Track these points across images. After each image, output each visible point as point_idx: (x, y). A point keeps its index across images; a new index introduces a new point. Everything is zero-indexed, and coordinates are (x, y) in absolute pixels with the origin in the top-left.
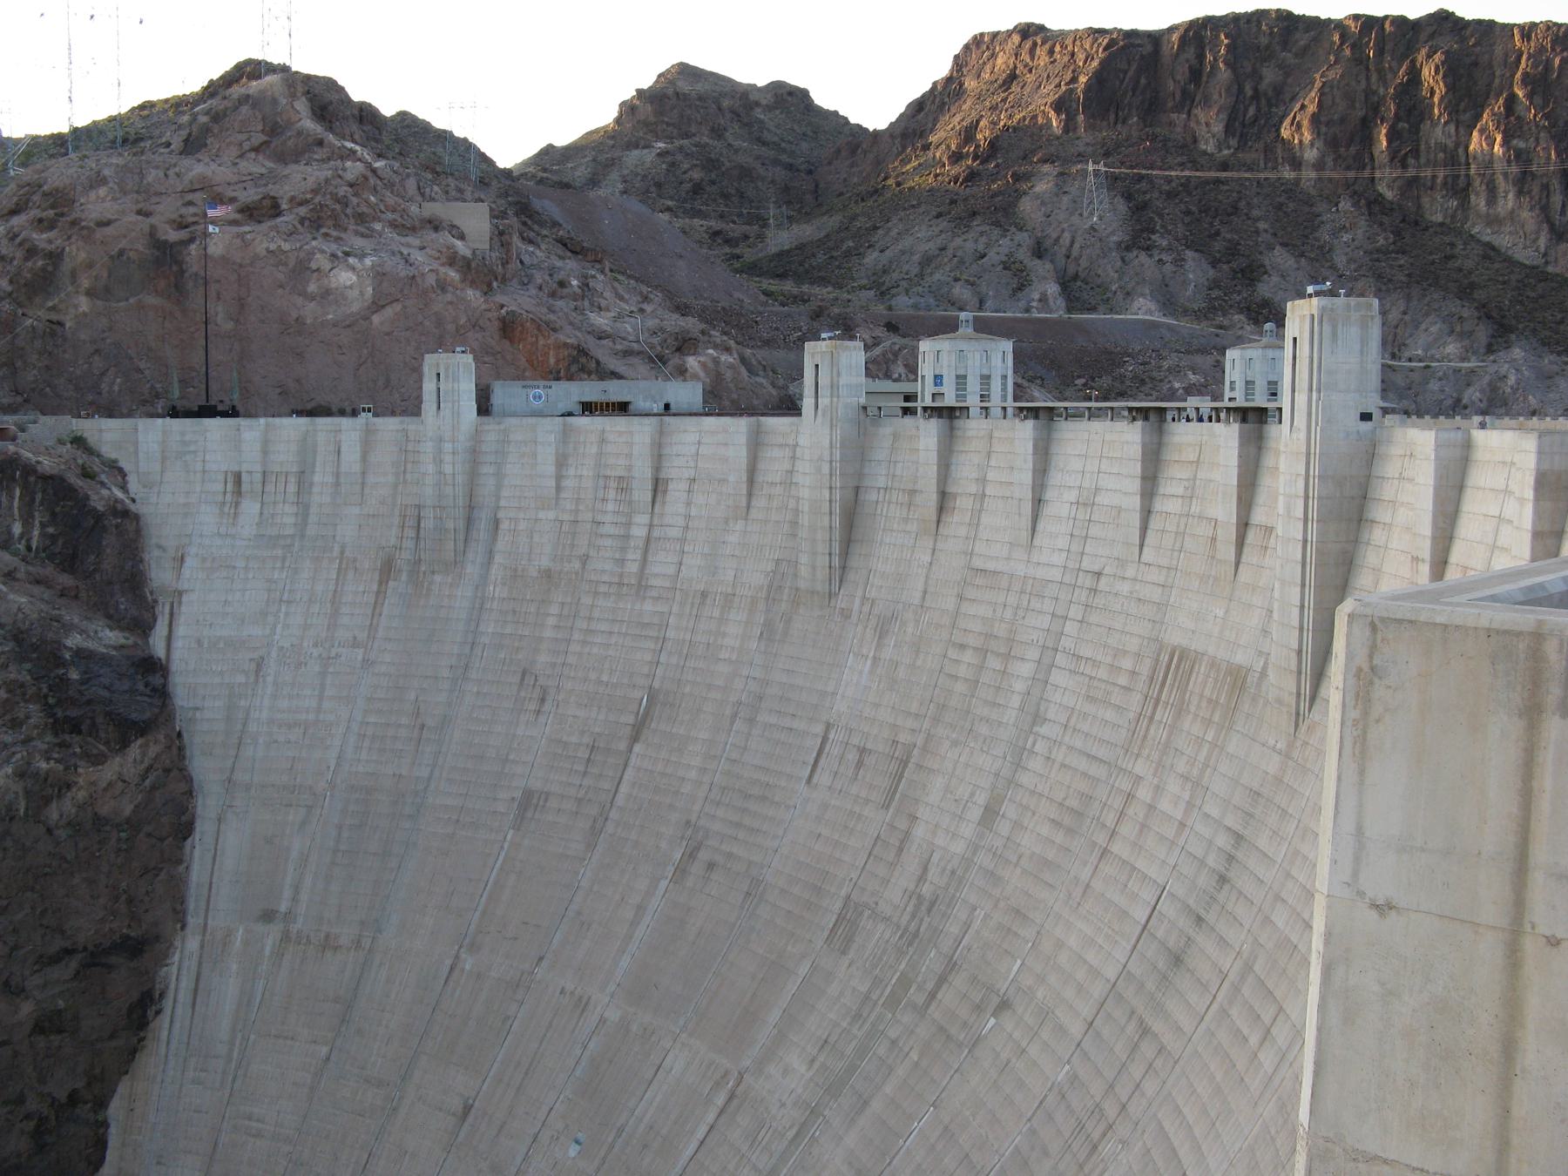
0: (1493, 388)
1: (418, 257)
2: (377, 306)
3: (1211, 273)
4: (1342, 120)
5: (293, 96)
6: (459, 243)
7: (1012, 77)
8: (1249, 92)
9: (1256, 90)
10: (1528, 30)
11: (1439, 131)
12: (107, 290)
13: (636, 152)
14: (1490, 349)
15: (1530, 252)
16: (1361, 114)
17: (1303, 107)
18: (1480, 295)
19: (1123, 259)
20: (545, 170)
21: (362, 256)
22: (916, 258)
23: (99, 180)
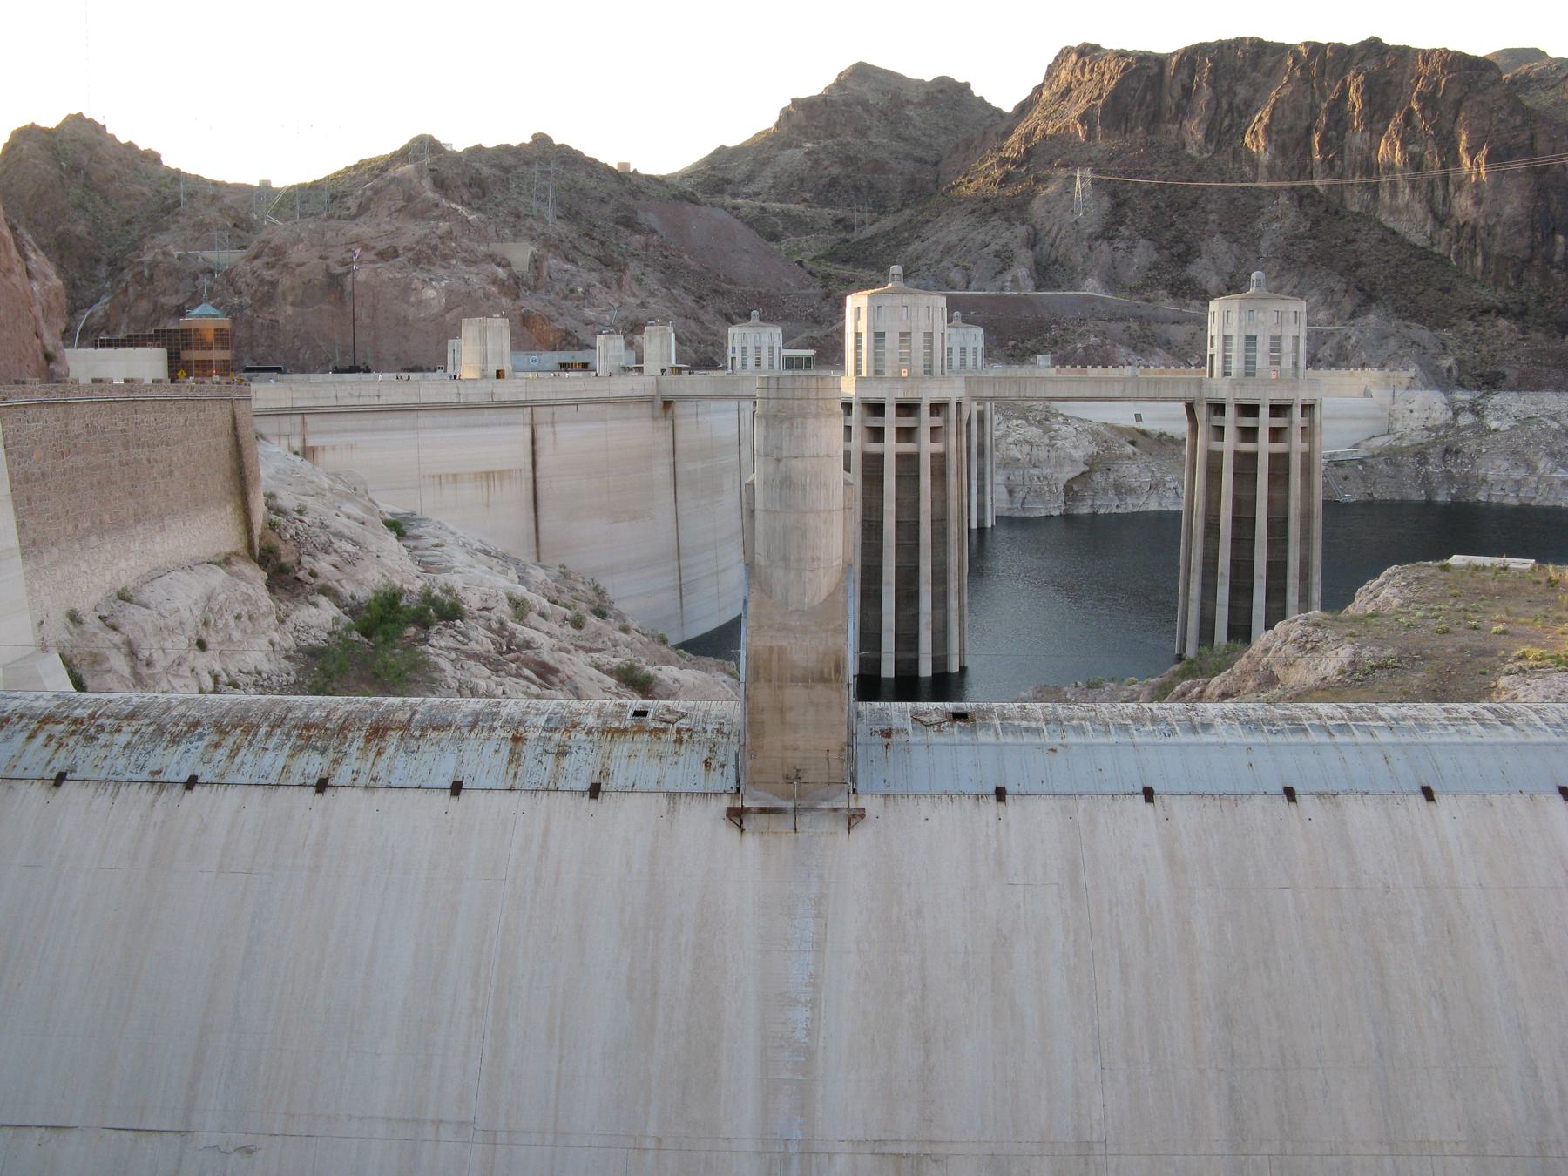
0: (1340, 346)
1: (474, 279)
2: (448, 309)
3: (1156, 256)
4: (1290, 129)
5: (421, 177)
6: (500, 270)
7: (1069, 90)
8: (1225, 106)
9: (1230, 104)
10: (1427, 55)
11: (1357, 137)
12: (302, 302)
13: (789, 152)
14: (1353, 315)
15: (1421, 236)
16: (1306, 123)
17: (1261, 119)
18: (1362, 272)
19: (1090, 248)
20: (713, 168)
21: (442, 279)
22: (940, 248)
23: (299, 240)
